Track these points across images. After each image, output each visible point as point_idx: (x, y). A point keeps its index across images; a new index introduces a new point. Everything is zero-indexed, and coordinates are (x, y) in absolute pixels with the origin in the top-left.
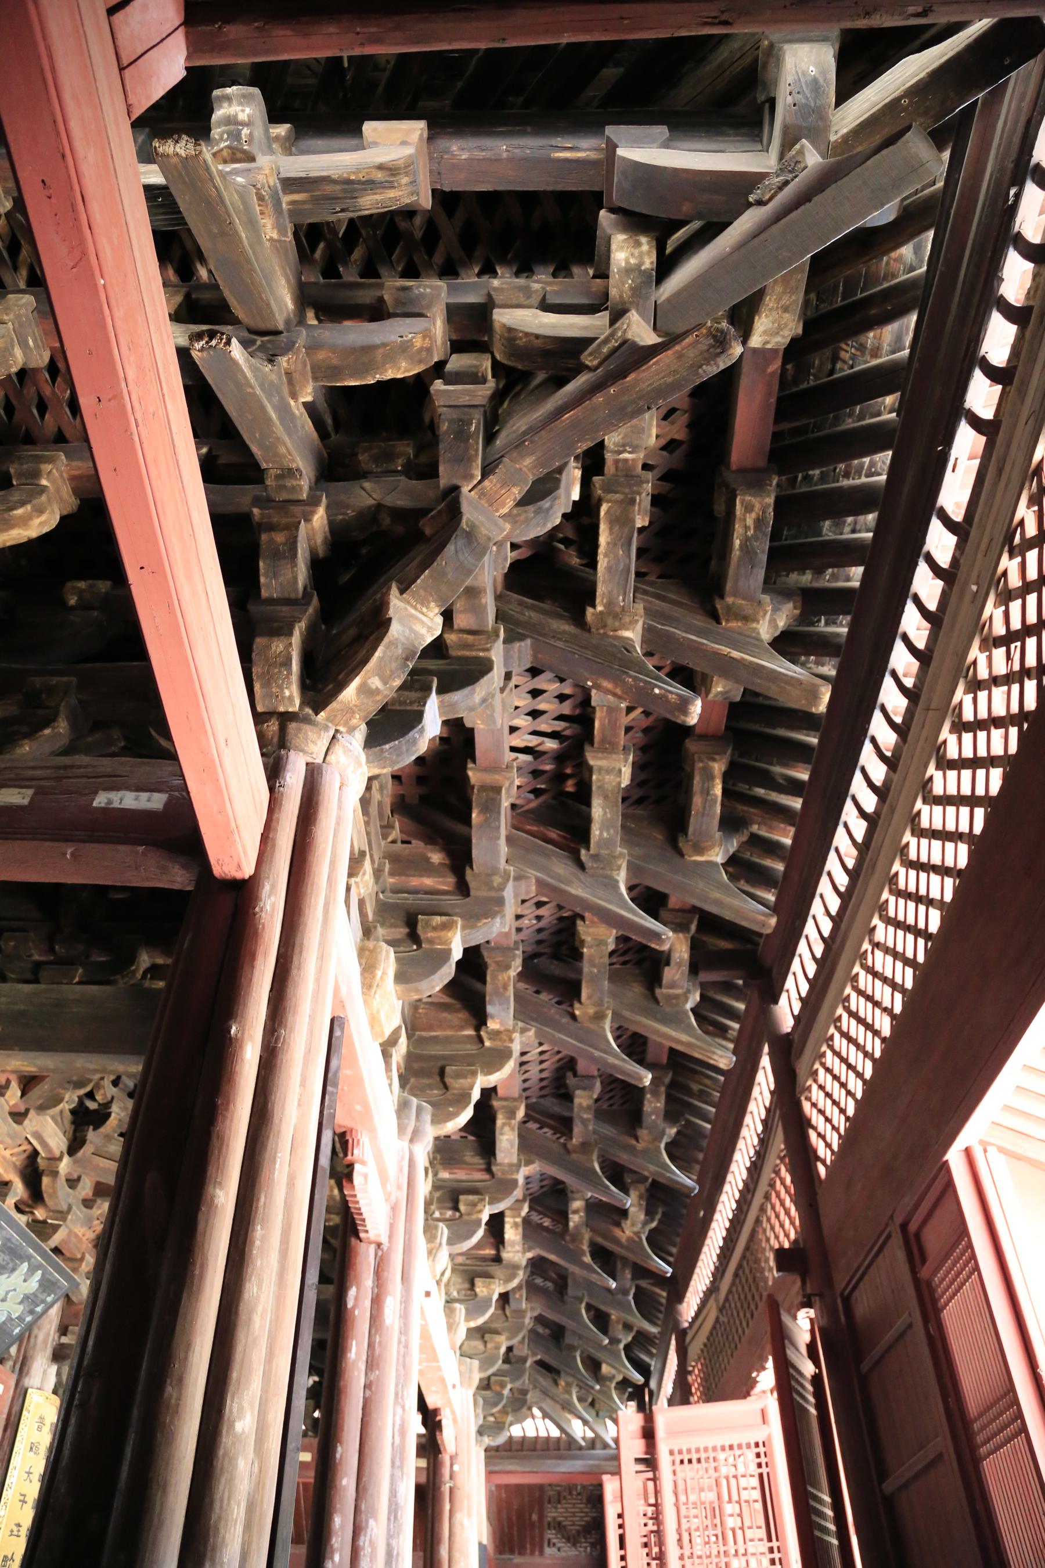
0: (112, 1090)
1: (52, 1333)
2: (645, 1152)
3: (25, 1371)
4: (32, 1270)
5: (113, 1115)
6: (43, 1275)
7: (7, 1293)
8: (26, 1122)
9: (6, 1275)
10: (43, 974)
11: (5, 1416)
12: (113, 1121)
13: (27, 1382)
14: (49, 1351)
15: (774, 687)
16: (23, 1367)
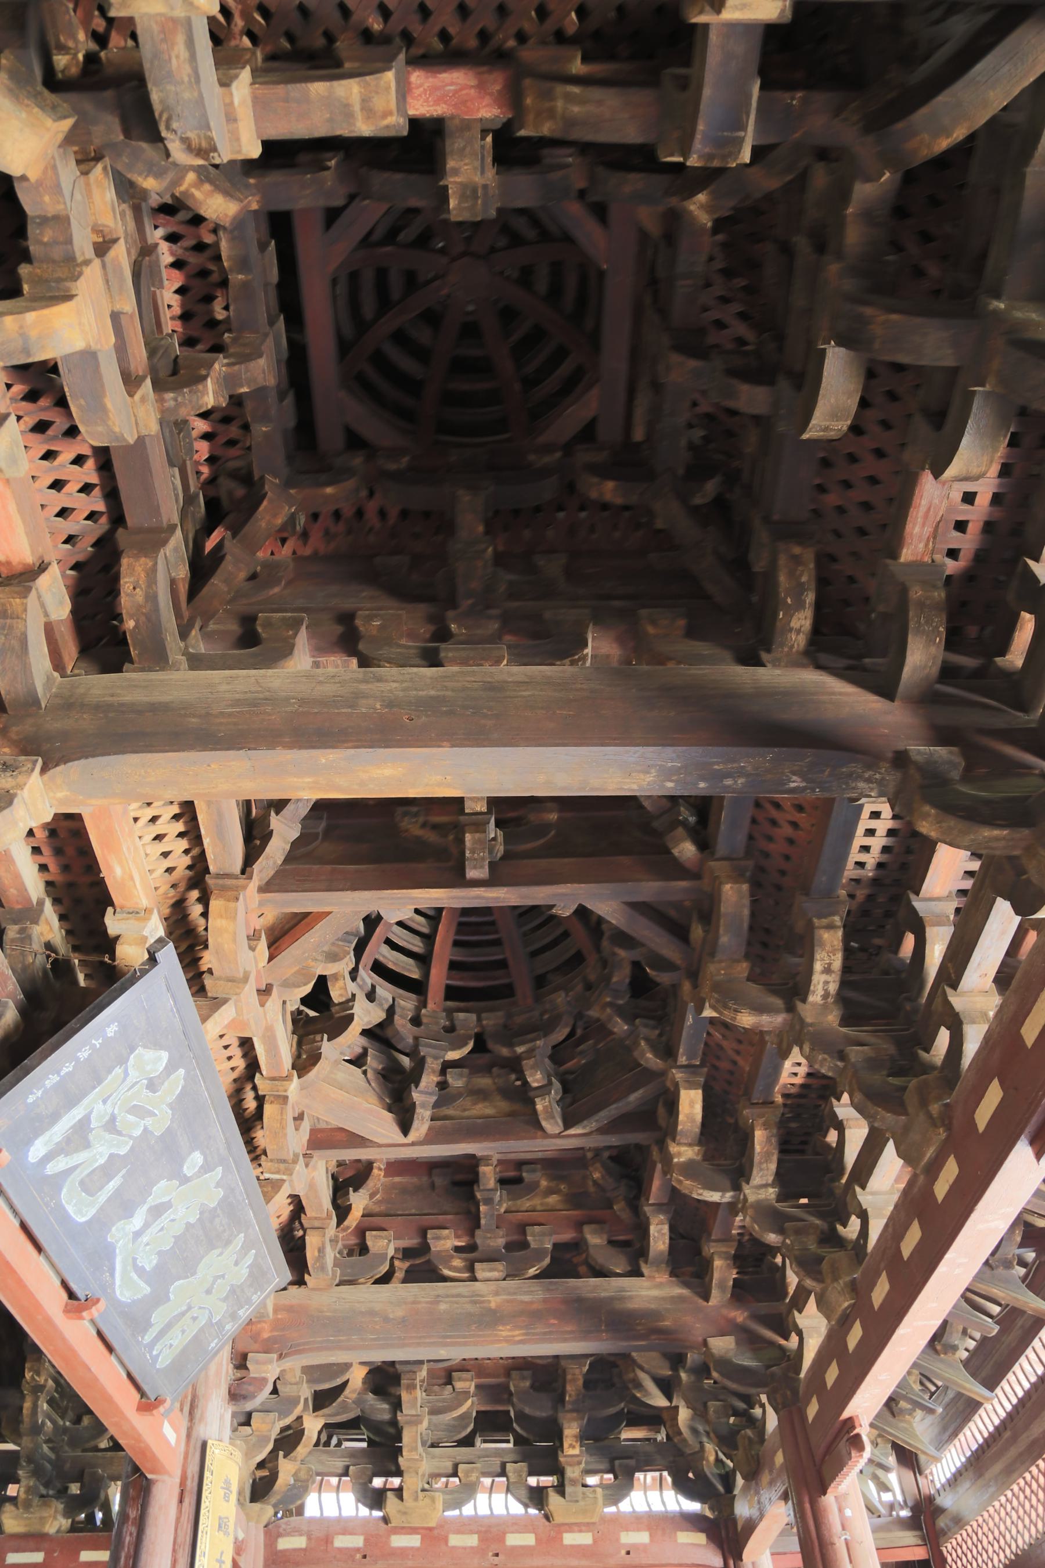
0: (352, 987)
1: (225, 1362)
3: (198, 1413)
5: (356, 1017)
6: (256, 1255)
7: (214, 1283)
8: (269, 1004)
9: (217, 1252)
11: (178, 1480)
13: (203, 1431)
14: (223, 1391)
16: (193, 1409)
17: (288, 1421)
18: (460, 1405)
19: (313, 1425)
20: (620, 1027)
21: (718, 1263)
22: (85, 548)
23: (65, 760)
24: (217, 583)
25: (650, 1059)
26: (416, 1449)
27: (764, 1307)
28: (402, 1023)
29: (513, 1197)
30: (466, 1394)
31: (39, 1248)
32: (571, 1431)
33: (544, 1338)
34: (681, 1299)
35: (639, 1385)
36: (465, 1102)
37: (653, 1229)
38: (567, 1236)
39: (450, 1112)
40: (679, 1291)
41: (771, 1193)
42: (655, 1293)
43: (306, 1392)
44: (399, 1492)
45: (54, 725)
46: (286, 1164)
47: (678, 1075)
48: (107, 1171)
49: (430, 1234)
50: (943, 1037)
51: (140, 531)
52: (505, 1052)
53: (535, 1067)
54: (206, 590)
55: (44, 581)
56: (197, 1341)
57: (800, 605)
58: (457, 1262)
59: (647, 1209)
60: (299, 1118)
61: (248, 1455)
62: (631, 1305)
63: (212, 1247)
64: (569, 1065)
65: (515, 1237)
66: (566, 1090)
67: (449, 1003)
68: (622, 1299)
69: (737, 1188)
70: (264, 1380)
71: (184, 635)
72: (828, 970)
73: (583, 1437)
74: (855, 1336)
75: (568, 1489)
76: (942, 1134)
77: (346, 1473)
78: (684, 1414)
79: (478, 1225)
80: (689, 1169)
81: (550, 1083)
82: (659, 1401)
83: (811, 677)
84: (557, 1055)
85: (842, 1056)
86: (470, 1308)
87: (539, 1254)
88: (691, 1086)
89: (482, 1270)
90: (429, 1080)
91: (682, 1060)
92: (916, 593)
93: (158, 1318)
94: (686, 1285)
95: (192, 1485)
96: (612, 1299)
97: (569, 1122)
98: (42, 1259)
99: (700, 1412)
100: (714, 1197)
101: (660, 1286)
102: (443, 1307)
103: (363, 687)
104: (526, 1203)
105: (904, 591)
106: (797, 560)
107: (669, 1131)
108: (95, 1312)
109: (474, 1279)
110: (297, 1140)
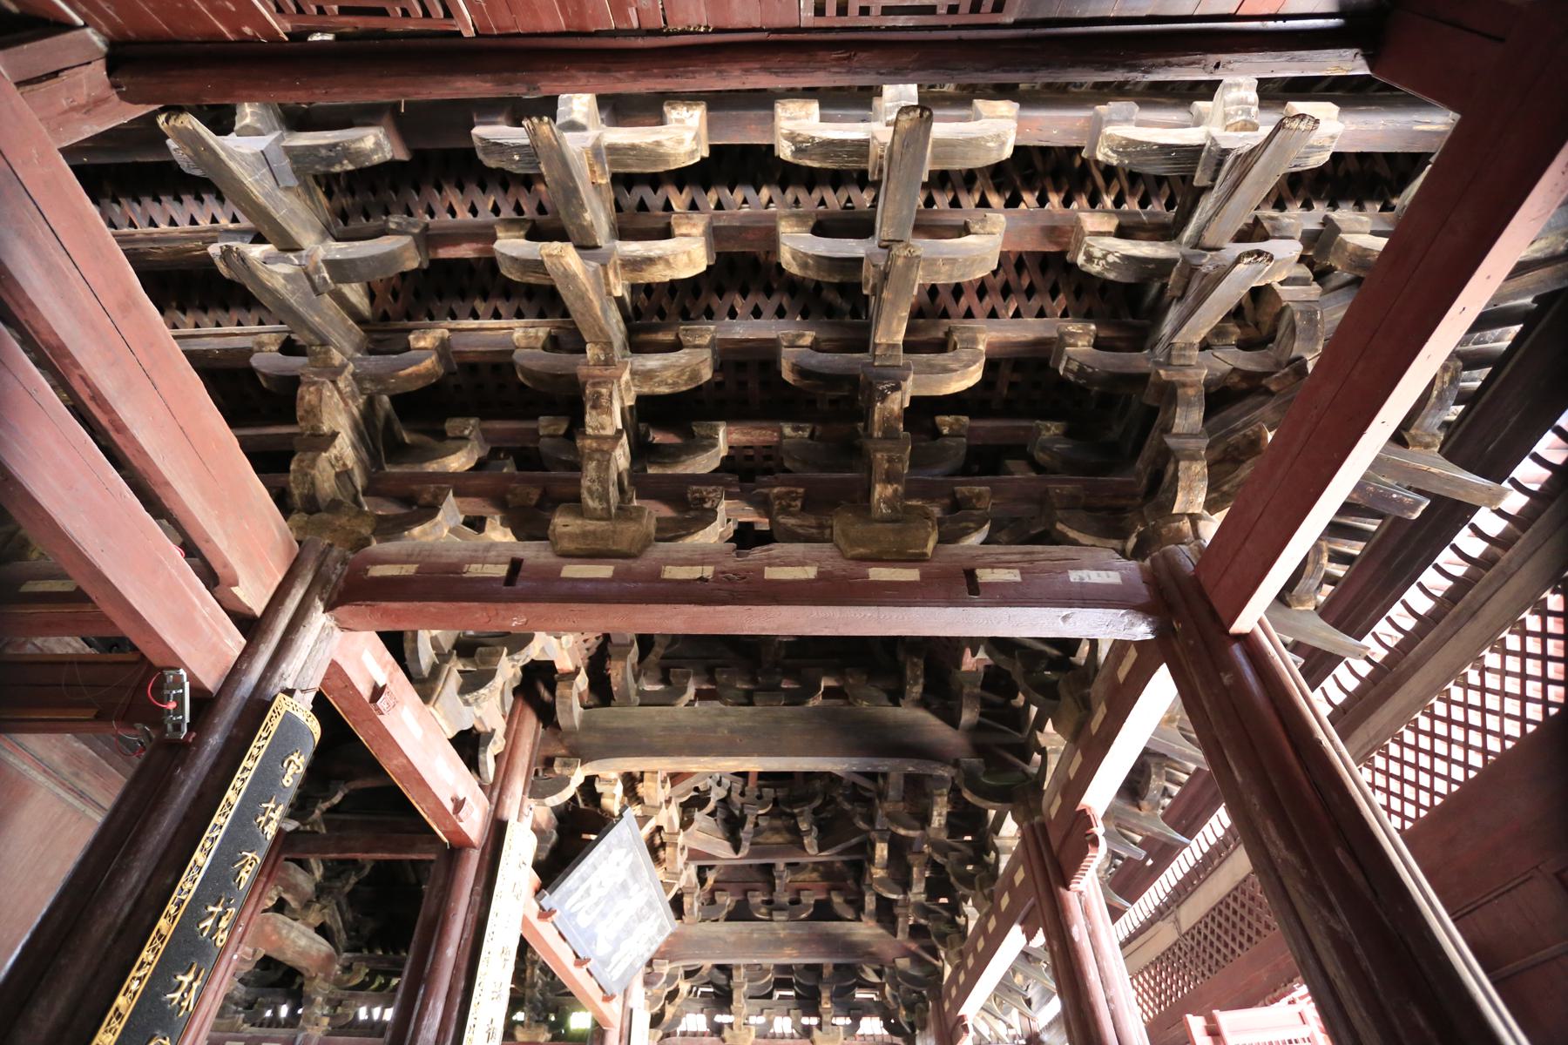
0: (710, 782)
2: (1146, 817)
4: (655, 920)
10: (756, 698)
11: (618, 1030)
12: (711, 806)
13: (631, 1004)
15: (1461, 492)
17: (671, 988)
18: (765, 977)
19: (684, 987)
20: (847, 806)
21: (900, 919)
22: (594, 650)
23: (591, 760)
24: (652, 658)
25: (862, 825)
26: (740, 1002)
27: (925, 942)
28: (735, 796)
29: (794, 873)
30: (768, 971)
31: (564, 939)
32: (825, 994)
33: (809, 955)
34: (881, 936)
35: (863, 971)
36: (767, 834)
37: (867, 898)
38: (822, 897)
39: (759, 840)
40: (881, 931)
41: (923, 897)
42: (868, 931)
43: (681, 972)
44: (731, 1025)
45: (585, 740)
46: (677, 875)
47: (874, 835)
48: (597, 904)
49: (749, 894)
50: (993, 854)
51: (618, 645)
52: (788, 810)
53: (804, 821)
54: (647, 661)
55: (579, 678)
56: (631, 965)
57: (916, 683)
58: (763, 910)
59: (864, 887)
60: (683, 849)
61: (651, 1007)
62: (855, 938)
63: (640, 921)
64: (823, 815)
65: (795, 896)
66: (820, 830)
67: (761, 782)
68: (850, 934)
69: (905, 893)
70: (662, 975)
71: (637, 679)
72: (940, 815)
73: (831, 998)
74: (962, 978)
75: (824, 1027)
76: (989, 904)
77: (702, 1011)
78: (887, 988)
79: (774, 890)
80: (881, 881)
81: (811, 830)
82: (874, 979)
83: (922, 715)
84: (815, 812)
85: (946, 856)
86: (769, 937)
87: (808, 906)
88: (882, 840)
89: (777, 916)
90: (749, 827)
91: (878, 827)
92: (966, 690)
93: (614, 960)
94: (884, 927)
95: (625, 1032)
96: (845, 934)
97: (821, 850)
98: (566, 945)
99: (896, 986)
100: (894, 897)
101: (871, 927)
102: (755, 936)
103: (720, 719)
104: (801, 877)
105: (962, 687)
106: (915, 665)
107: (871, 860)
108: (589, 965)
109: (771, 920)
110: (681, 859)
